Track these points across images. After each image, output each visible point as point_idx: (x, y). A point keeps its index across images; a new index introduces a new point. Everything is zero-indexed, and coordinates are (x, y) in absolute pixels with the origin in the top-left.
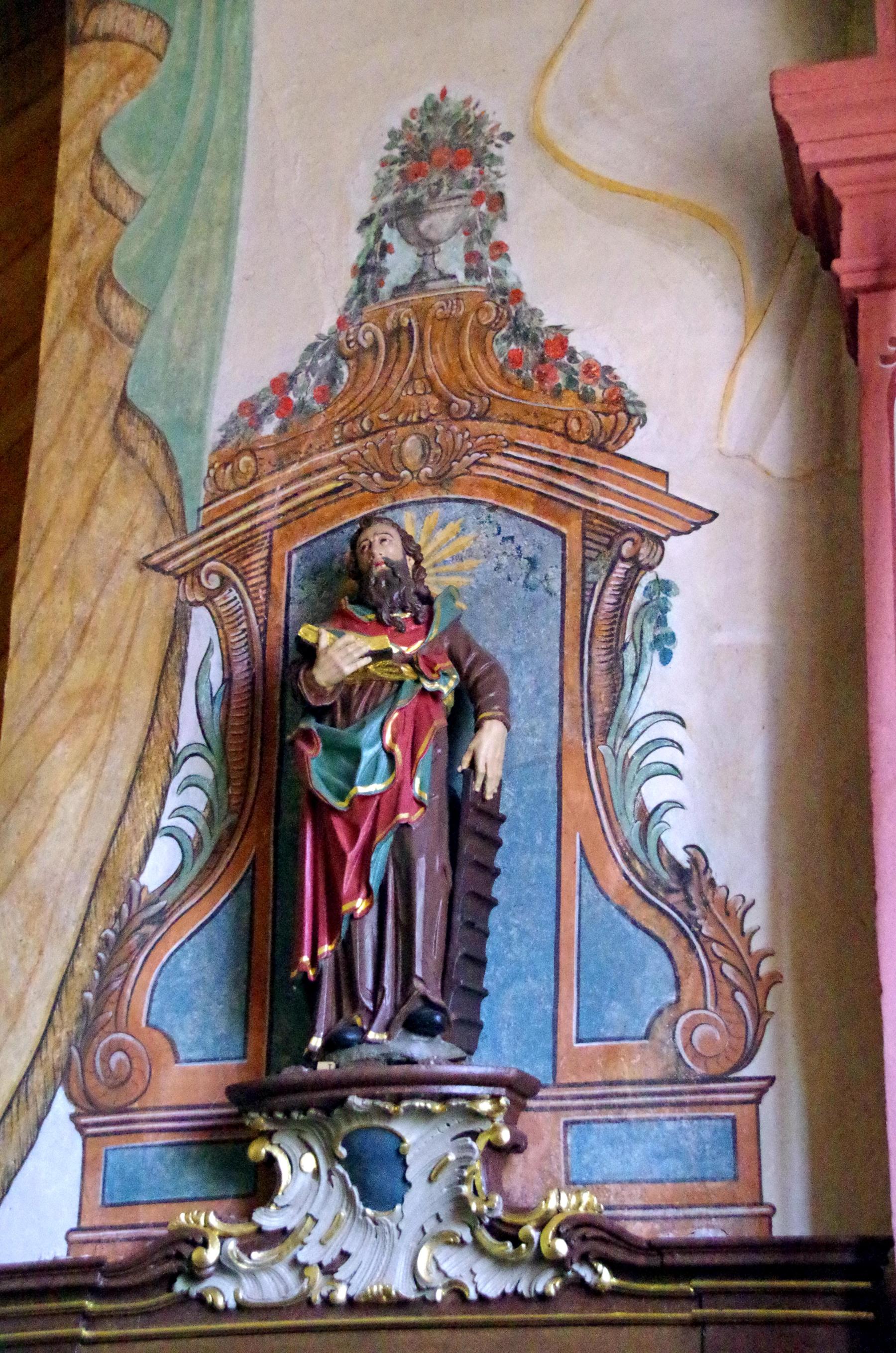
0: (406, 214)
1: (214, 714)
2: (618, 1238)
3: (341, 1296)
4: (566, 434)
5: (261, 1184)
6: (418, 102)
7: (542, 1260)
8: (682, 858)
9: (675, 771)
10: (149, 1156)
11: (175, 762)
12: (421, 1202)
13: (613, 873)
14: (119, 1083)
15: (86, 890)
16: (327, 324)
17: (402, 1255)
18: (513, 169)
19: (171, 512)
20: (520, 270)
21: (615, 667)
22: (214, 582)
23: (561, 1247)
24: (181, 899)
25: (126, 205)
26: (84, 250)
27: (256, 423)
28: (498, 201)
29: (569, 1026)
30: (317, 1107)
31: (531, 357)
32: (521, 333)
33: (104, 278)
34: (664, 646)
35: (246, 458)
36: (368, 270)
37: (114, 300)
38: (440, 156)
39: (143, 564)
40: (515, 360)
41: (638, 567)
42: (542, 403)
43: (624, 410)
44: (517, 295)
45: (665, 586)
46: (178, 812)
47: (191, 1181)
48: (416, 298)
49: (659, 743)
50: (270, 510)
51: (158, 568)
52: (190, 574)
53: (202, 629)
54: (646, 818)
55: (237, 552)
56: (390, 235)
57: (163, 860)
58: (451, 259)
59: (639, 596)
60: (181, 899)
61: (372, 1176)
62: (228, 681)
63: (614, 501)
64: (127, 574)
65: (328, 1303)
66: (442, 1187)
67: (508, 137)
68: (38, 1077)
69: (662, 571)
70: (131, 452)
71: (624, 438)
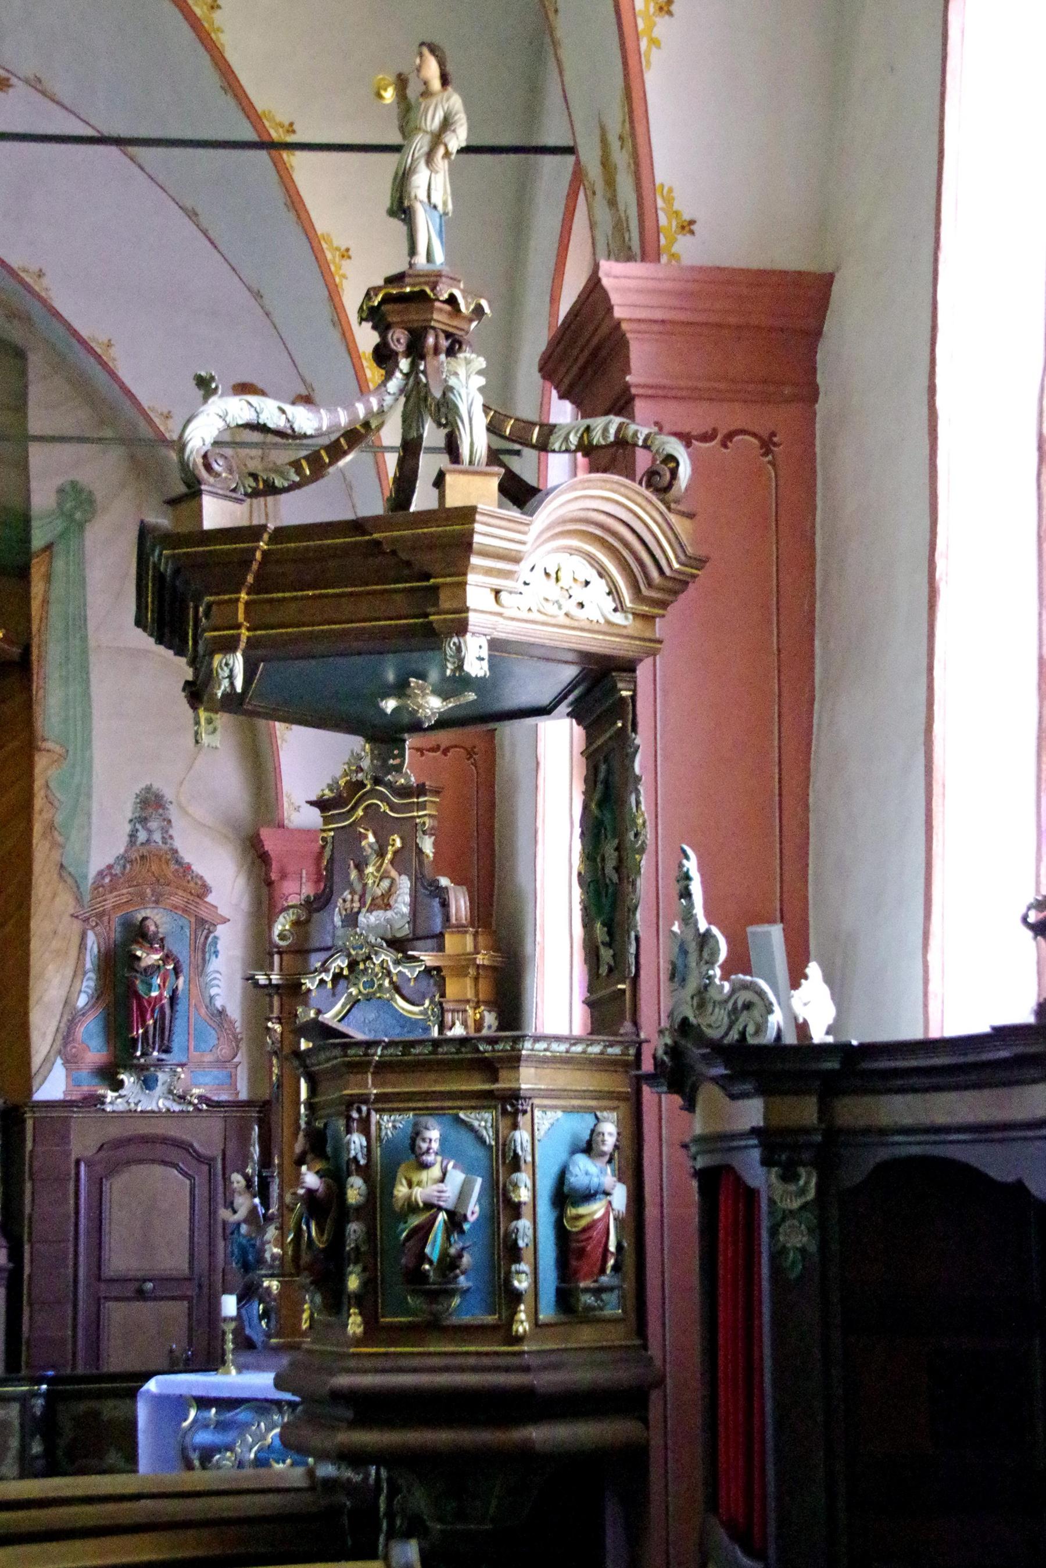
1: (96, 962)
2: (209, 1099)
3: (139, 1109)
4: (191, 893)
6: (144, 786)
7: (190, 1103)
8: (220, 1009)
9: (218, 986)
10: (84, 1074)
11: (85, 973)
12: (160, 1089)
13: (203, 1011)
14: (75, 1056)
15: (61, 1007)
16: (122, 851)
17: (157, 1101)
18: (173, 813)
19: (79, 899)
20: (177, 844)
21: (204, 959)
22: (94, 924)
23: (196, 1101)
24: (88, 1010)
25: (56, 803)
26: (46, 816)
27: (103, 878)
28: (170, 821)
29: (192, 1048)
31: (181, 870)
32: (178, 862)
33: (51, 826)
34: (216, 953)
35: (101, 889)
36: (133, 836)
37: (56, 833)
38: (151, 804)
39: (72, 916)
40: (177, 871)
41: (210, 932)
42: (185, 884)
43: (205, 889)
44: (176, 852)
45: (216, 938)
46: (87, 987)
47: (96, 1081)
48: (147, 847)
49: (215, 978)
50: (109, 905)
51: (77, 917)
52: (86, 920)
53: (91, 937)
54: (211, 998)
55: (100, 915)
56: (138, 826)
58: (157, 837)
59: (210, 939)
60: (88, 1010)
61: (148, 1084)
62: (99, 952)
63: (204, 914)
64: (66, 918)
65: (135, 1111)
66: (165, 1087)
67: (171, 803)
68: (52, 1054)
69: (216, 933)
70: (65, 881)
71: (206, 896)
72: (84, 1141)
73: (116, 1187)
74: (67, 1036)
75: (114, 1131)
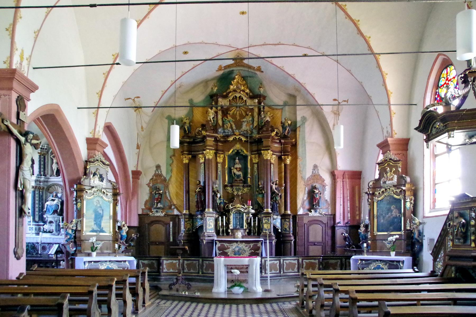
0: (314, 169)
5: (311, 212)
10: (306, 210)
12: (318, 212)
17: (317, 214)
18: (319, 168)
20: (320, 173)
30: (313, 208)
33: (300, 171)
36: (313, 172)
38: (315, 167)
43: (324, 181)
53: (306, 188)
57: (305, 198)
61: (316, 212)
72: (306, 221)
73: (311, 228)
74: (303, 204)
75: (310, 219)
